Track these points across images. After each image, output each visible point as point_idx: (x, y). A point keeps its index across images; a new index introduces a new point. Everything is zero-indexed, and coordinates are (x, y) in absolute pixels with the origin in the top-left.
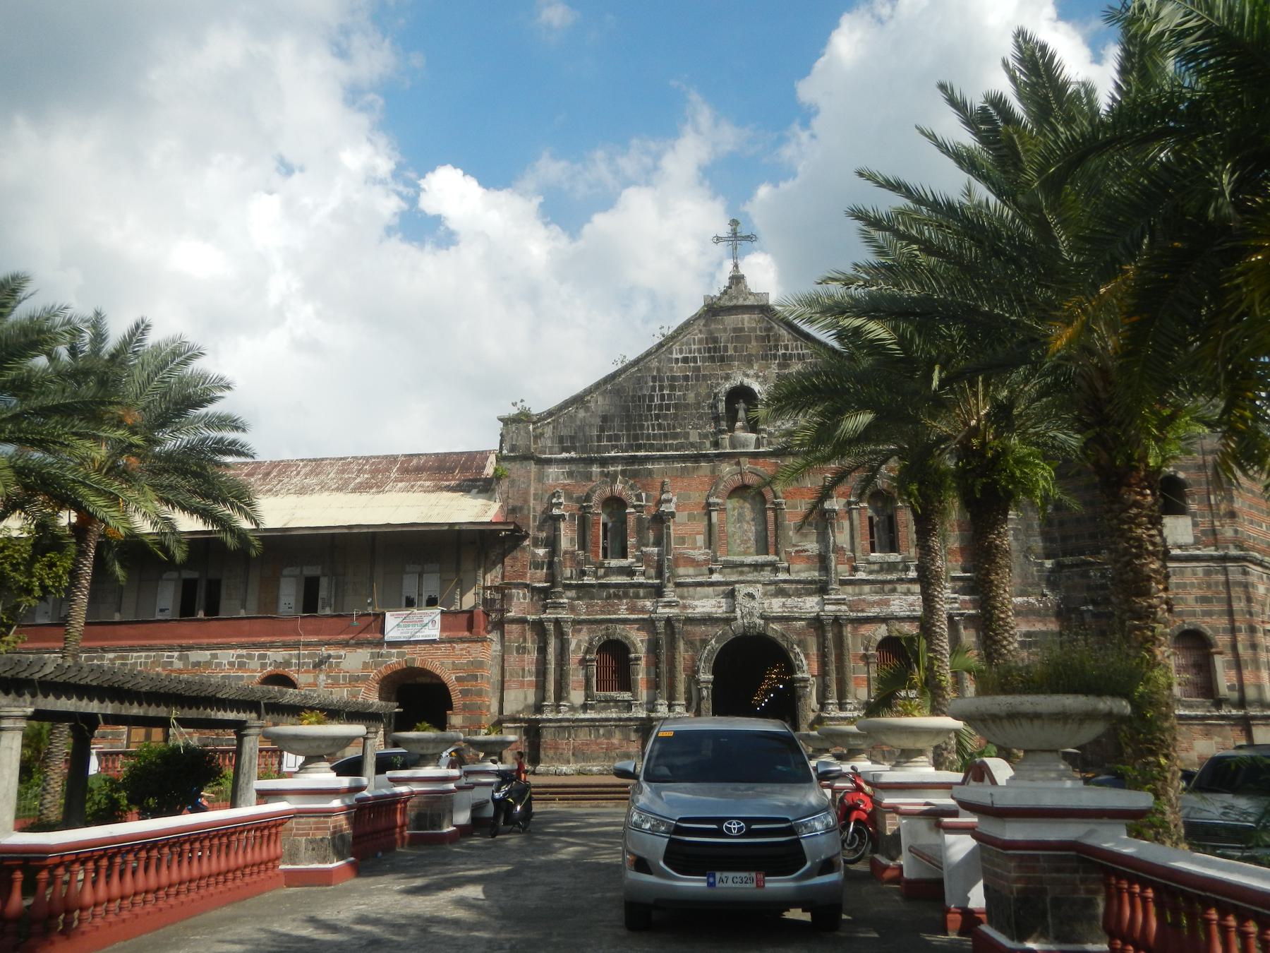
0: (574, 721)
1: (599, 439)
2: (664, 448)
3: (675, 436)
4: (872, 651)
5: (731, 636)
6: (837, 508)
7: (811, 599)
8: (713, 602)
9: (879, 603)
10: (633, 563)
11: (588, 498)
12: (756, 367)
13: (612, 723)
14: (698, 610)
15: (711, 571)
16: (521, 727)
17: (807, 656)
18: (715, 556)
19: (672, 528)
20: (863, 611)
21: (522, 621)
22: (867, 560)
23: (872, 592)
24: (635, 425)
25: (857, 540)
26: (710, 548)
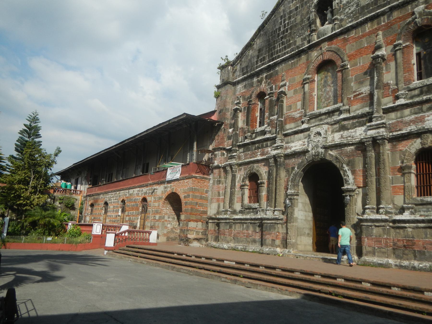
0: (234, 219)
1: (257, 62)
2: (285, 54)
3: (289, 46)
5: (305, 162)
7: (360, 128)
8: (301, 142)
9: (414, 122)
13: (249, 221)
15: (303, 123)
16: (214, 222)
17: (353, 172)
18: (305, 113)
19: (285, 101)
20: (400, 130)
21: (218, 167)
22: (408, 87)
23: (412, 114)
26: (303, 109)
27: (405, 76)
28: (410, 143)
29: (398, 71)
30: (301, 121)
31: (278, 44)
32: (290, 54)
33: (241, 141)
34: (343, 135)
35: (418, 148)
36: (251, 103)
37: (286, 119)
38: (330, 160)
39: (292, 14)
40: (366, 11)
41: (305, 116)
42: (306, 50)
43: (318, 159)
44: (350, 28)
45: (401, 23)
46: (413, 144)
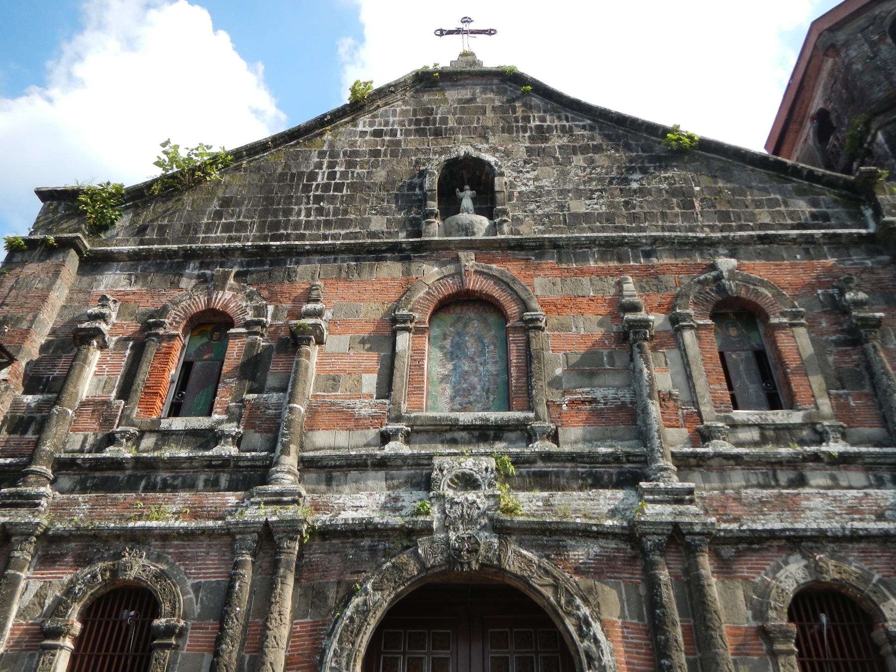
1: (209, 228)
2: (325, 237)
4: (778, 619)
6: (651, 317)
7: (609, 493)
10: (220, 422)
11: (163, 311)
12: (493, 140)
14: (349, 515)
15: (385, 438)
24: (277, 210)
25: (701, 383)
27: (715, 390)
28: (772, 563)
29: (695, 374)
30: (377, 430)
31: (303, 207)
32: (352, 242)
33: (77, 447)
34: (552, 501)
35: (802, 581)
36: (161, 332)
37: (317, 412)
38: (519, 573)
39: (358, 159)
40: (584, 225)
41: (398, 419)
42: (405, 250)
43: (475, 566)
44: (547, 243)
45: (681, 276)
46: (779, 568)
